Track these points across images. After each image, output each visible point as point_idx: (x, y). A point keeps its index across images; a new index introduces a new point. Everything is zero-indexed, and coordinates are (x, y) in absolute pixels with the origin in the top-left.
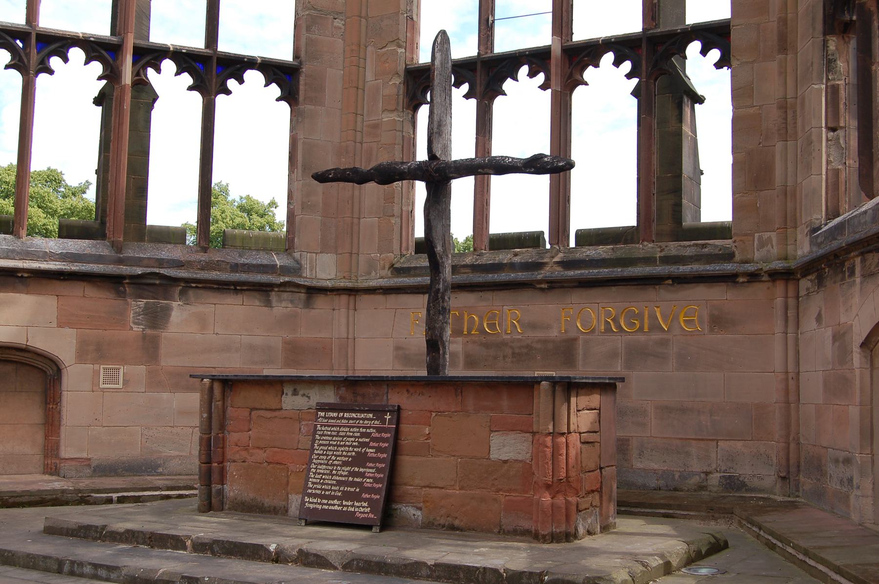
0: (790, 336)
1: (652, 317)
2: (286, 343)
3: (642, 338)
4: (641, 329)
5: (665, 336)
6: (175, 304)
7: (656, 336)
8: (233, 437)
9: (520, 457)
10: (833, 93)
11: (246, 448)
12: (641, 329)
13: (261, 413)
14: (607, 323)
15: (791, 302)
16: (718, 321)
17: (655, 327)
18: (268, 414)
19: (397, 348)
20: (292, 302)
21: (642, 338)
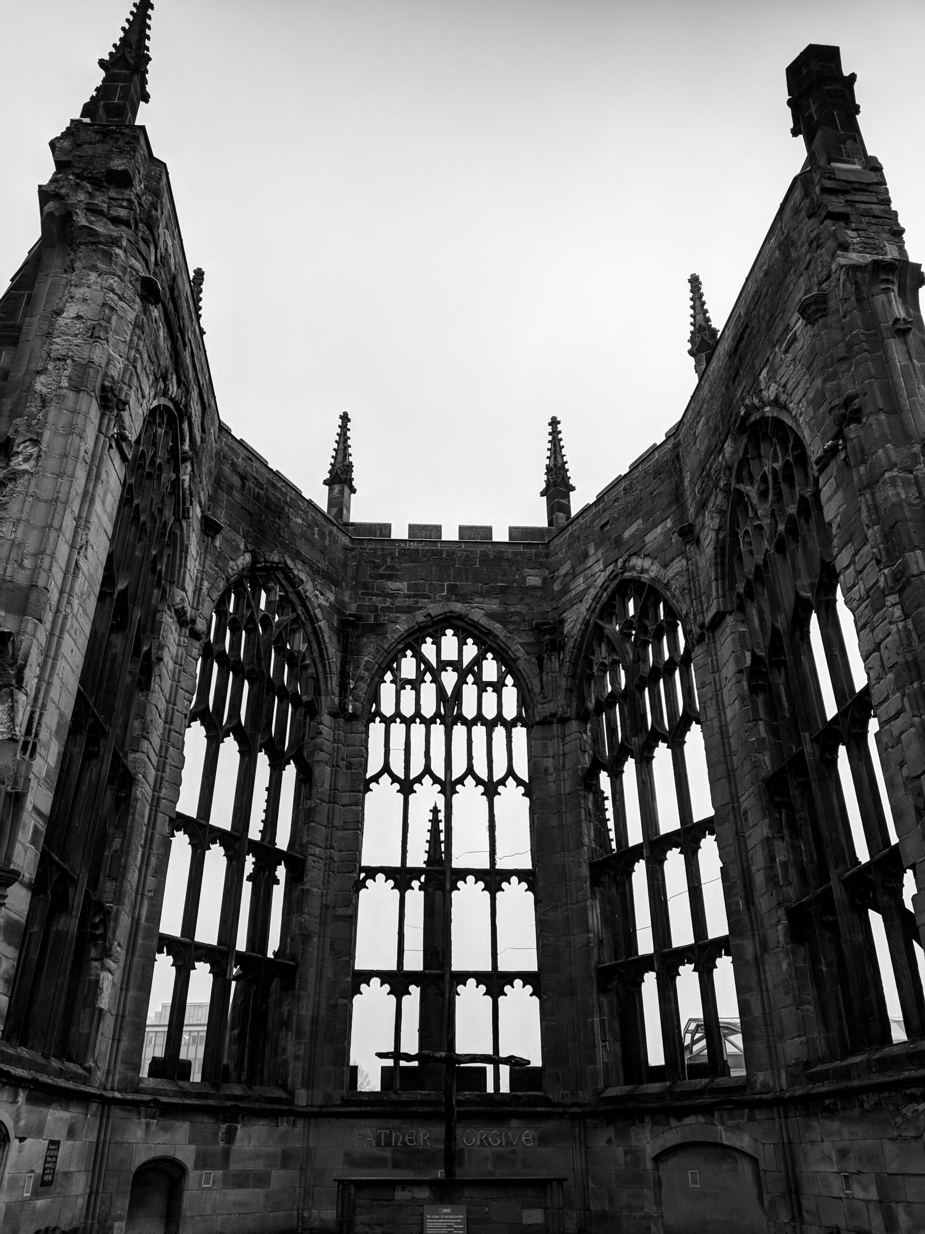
0: (583, 1149)
1: (507, 1137)
2: (283, 1151)
3: (502, 1149)
4: (501, 1143)
5: (515, 1148)
6: (239, 1126)
7: (509, 1149)
8: (359, 1219)
9: (538, 1222)
10: (602, 1022)
11: (369, 1225)
12: (501, 1143)
13: (380, 1202)
14: (481, 1140)
15: (582, 1130)
16: (543, 1140)
17: (509, 1143)
18: (385, 1203)
19: (346, 1154)
20: (287, 1122)
21: (502, 1149)
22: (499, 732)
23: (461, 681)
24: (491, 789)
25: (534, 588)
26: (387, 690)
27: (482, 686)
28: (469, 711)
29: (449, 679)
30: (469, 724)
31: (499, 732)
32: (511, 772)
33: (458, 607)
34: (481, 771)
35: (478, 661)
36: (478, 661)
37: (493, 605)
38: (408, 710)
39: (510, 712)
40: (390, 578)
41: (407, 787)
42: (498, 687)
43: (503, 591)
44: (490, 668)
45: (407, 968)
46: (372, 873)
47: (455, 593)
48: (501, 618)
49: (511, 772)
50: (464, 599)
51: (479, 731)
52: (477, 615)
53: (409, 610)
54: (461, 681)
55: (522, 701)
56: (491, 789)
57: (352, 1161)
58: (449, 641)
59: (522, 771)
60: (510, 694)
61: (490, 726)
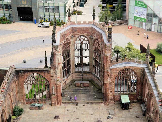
22: (87, 45)
23: (83, 40)
24: (86, 50)
25: (90, 32)
26: (76, 42)
27: (85, 41)
28: (84, 43)
29: (82, 40)
30: (84, 44)
31: (87, 45)
32: (88, 48)
33: (83, 34)
34: (85, 48)
35: (85, 38)
36: (85, 38)
37: (86, 34)
38: (78, 43)
39: (88, 43)
40: (76, 31)
41: (78, 50)
42: (87, 41)
43: (87, 32)
44: (86, 39)
45: (79, 62)
46: (76, 57)
47: (82, 33)
48: (87, 35)
49: (88, 48)
50: (83, 33)
51: (85, 45)
52: (84, 35)
53: (78, 35)
54: (83, 40)
55: (89, 42)
56: (86, 50)
57: (76, 76)
58: (82, 36)
59: (89, 48)
60: (88, 41)
61: (86, 44)
